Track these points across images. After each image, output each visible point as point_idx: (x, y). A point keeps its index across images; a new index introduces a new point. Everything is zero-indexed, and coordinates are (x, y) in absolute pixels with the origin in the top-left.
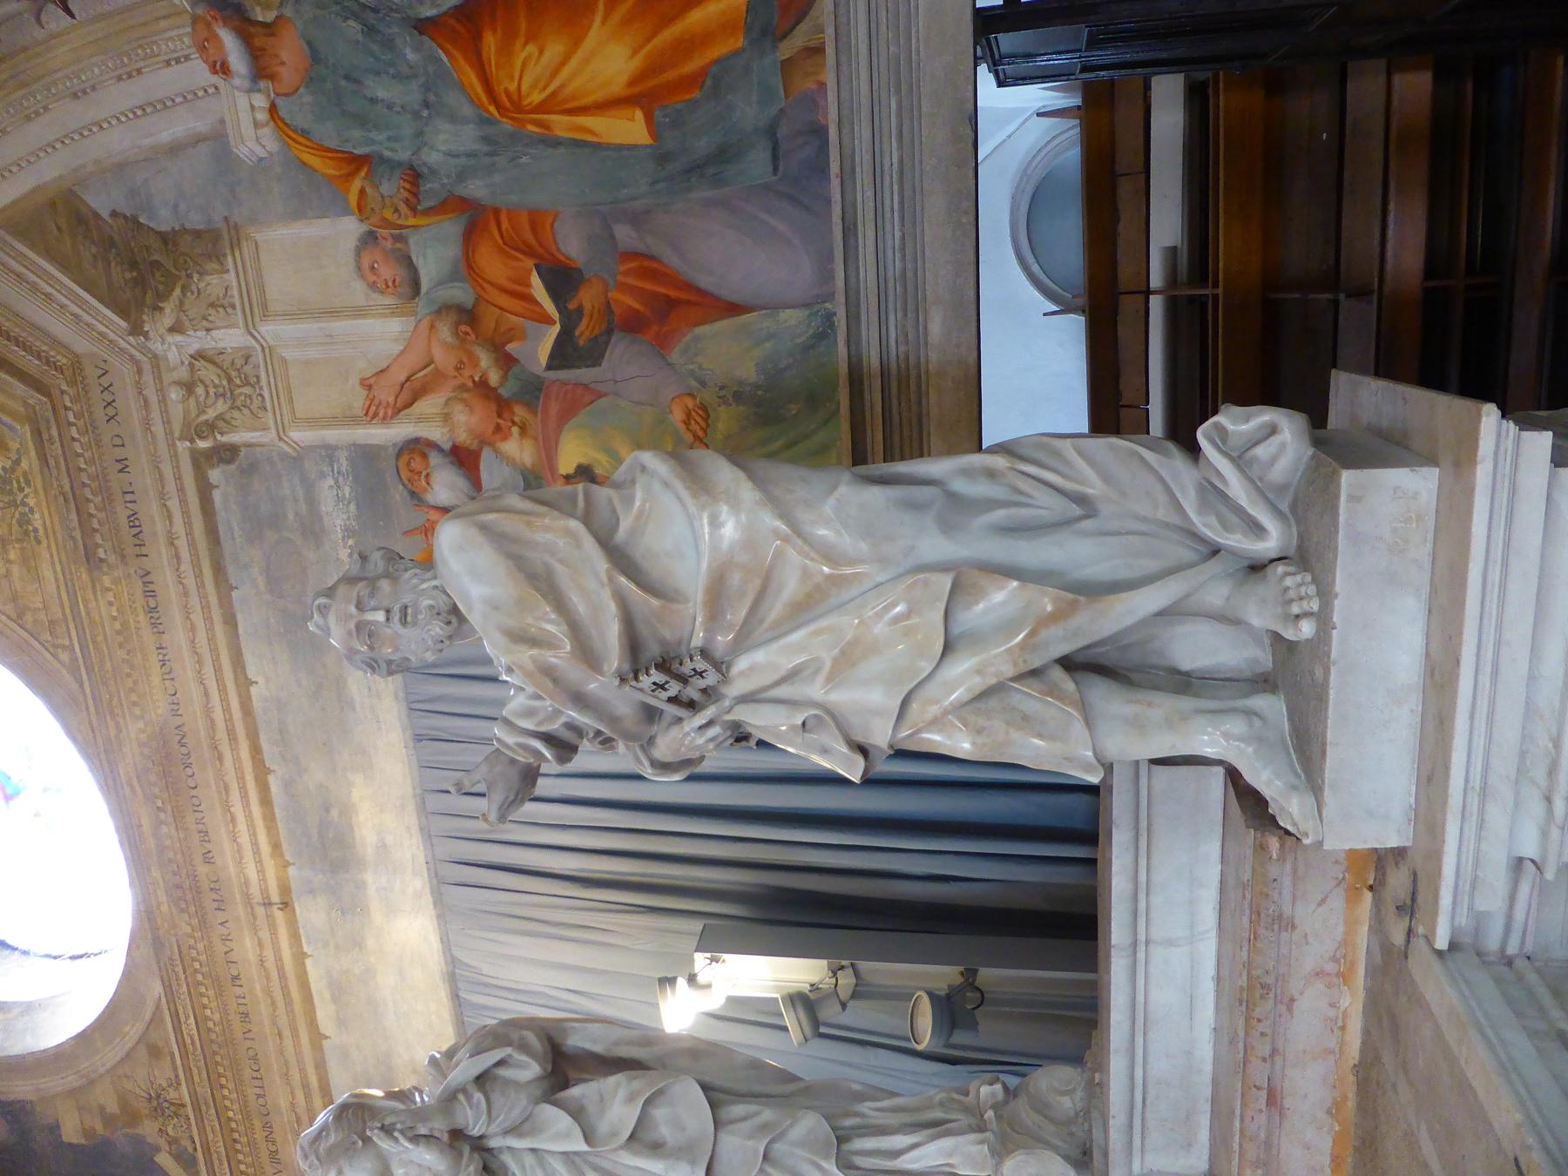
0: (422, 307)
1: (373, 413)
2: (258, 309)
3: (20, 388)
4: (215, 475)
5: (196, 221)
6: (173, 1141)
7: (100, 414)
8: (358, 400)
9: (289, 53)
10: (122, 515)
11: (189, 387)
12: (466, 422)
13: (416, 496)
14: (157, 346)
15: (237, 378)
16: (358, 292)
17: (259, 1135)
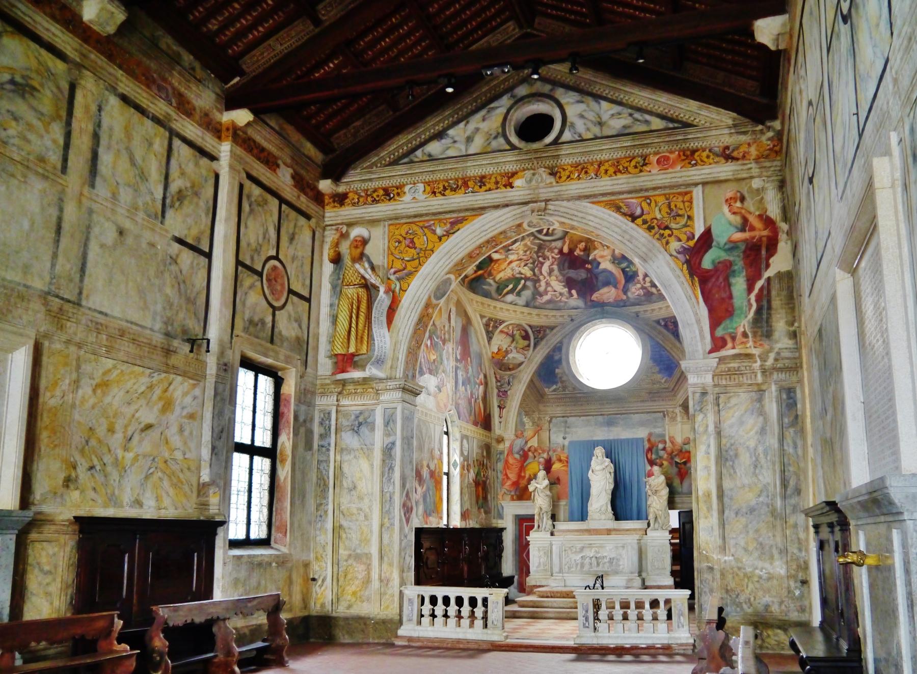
1: (670, 438)
2: (683, 423)
12: (669, 449)
15: (673, 419)
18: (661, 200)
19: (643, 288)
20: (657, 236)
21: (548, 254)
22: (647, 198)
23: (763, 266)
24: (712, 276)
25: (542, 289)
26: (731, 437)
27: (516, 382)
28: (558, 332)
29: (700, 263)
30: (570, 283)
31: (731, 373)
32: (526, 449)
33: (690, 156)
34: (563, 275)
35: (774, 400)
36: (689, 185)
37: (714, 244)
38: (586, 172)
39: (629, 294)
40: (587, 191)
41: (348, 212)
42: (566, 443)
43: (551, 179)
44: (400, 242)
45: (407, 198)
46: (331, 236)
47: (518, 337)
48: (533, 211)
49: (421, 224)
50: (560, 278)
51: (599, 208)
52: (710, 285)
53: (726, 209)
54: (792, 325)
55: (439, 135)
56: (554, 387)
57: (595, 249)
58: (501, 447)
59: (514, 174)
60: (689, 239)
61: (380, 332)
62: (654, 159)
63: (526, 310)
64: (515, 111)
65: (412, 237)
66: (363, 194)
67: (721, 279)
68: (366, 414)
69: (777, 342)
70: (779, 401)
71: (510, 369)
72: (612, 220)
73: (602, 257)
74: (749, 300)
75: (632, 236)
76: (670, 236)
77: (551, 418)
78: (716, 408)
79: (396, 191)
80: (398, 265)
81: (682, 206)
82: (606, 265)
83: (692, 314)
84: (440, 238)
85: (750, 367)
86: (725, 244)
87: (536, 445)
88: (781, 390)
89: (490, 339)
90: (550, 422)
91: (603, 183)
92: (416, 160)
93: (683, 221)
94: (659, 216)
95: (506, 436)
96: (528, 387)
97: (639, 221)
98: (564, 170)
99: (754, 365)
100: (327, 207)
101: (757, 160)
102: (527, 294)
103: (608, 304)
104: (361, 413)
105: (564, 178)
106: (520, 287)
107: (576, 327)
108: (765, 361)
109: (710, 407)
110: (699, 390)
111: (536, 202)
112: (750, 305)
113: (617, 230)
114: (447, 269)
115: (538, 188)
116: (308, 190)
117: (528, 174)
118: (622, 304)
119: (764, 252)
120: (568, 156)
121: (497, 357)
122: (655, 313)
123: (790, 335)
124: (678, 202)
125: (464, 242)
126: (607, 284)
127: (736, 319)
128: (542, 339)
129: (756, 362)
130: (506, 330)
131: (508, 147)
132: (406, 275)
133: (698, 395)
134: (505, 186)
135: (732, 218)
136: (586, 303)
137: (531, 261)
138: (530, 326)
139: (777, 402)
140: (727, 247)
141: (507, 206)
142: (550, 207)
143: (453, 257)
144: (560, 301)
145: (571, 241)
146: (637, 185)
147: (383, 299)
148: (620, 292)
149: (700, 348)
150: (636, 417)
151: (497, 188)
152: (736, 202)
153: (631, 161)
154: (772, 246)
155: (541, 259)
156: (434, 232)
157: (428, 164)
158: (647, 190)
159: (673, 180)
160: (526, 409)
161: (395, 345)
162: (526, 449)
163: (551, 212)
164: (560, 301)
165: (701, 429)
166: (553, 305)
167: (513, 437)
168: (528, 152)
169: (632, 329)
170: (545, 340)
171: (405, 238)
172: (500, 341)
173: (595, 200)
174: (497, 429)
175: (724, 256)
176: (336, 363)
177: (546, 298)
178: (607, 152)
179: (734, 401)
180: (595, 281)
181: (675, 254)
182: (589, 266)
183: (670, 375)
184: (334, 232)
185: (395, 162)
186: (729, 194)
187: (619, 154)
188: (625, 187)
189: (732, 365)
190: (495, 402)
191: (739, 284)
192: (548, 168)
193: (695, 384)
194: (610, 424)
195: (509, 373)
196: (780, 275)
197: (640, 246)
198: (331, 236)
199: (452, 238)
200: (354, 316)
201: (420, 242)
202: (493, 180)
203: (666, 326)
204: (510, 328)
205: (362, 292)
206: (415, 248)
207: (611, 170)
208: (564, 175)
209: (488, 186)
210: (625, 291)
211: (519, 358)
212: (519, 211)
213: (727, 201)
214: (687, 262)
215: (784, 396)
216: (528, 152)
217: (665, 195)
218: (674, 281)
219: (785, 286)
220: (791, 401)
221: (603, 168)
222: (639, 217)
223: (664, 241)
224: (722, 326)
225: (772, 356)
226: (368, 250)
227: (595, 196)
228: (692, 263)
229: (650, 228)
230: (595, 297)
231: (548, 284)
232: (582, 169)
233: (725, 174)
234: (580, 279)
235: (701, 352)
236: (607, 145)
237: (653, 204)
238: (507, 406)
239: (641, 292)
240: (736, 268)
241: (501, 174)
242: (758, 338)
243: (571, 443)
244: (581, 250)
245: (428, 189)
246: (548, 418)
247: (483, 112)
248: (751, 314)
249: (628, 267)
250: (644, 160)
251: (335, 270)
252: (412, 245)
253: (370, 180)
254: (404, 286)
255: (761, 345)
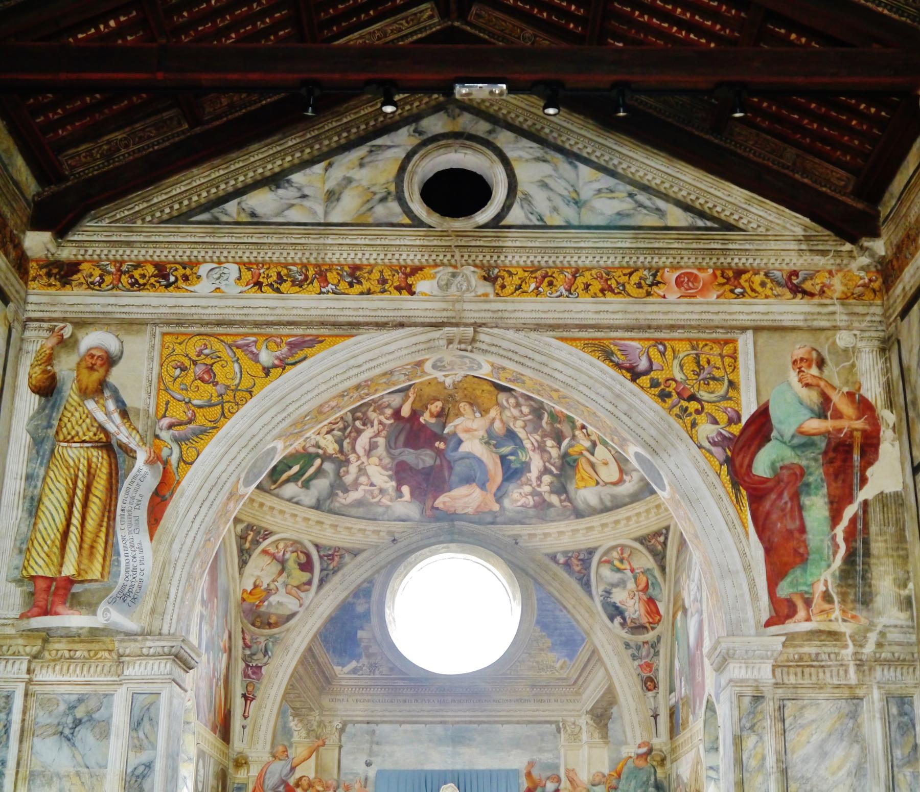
0: (590, 786)
1: (567, 770)
3: (575, 677)
4: (554, 726)
5: (610, 734)
6: (361, 668)
7: (568, 698)
8: (570, 767)
9: (641, 763)
10: (545, 698)
11: (574, 724)
13: (548, 778)
14: (583, 717)
15: (575, 737)
16: (593, 771)
17: (367, 698)
18: (684, 349)
19: (534, 493)
20: (676, 410)
21: (372, 415)
22: (660, 341)
23: (856, 480)
24: (770, 490)
25: (349, 479)
26: (805, 780)
27: (277, 651)
28: (367, 560)
29: (750, 466)
30: (401, 473)
31: (802, 664)
32: (292, 782)
33: (733, 280)
34: (392, 457)
35: (878, 715)
36: (732, 329)
37: (774, 434)
38: (551, 284)
39: (507, 503)
40: (551, 318)
41: (76, 299)
42: (372, 773)
43: (487, 288)
44: (183, 369)
45: (203, 287)
46: (37, 341)
47: (292, 565)
48: (450, 342)
49: (229, 340)
50: (387, 461)
51: (574, 350)
52: (767, 505)
53: (793, 376)
54: (905, 586)
55: (275, 180)
56: (354, 664)
57: (459, 414)
58: (241, 776)
59: (416, 270)
60: (731, 421)
61: (131, 535)
62: (671, 276)
63: (314, 515)
64: (423, 157)
65: (209, 361)
66: (112, 269)
67: (786, 497)
68: (93, 703)
69: (880, 614)
70: (887, 721)
71: (270, 625)
72: (595, 372)
73: (468, 431)
74: (834, 538)
75: (630, 405)
76: (698, 412)
77: (345, 724)
78: (780, 725)
79: (181, 271)
80: (178, 412)
81: (719, 363)
82: (473, 446)
83: (736, 554)
84: (267, 371)
85: (837, 654)
86: (793, 437)
87: (312, 775)
88: (888, 698)
89: (243, 563)
90: (342, 731)
91: (580, 307)
92: (225, 219)
93: (722, 389)
94: (679, 376)
95: (252, 755)
96: (303, 661)
97: (645, 380)
98: (510, 274)
99: (844, 652)
100: (32, 284)
101: (844, 299)
102: (321, 485)
103: (464, 517)
104: (80, 700)
105: (510, 289)
106: (311, 470)
107: (401, 554)
108: (861, 646)
109: (768, 723)
110: (749, 692)
111: (457, 325)
112: (836, 547)
113: (603, 391)
114: (277, 430)
115: (460, 300)
116: (10, 247)
117: (444, 273)
118: (489, 519)
119: (856, 456)
120: (517, 251)
121: (251, 600)
122: (550, 541)
123: (901, 603)
124: (712, 354)
125: (314, 382)
126: (468, 480)
127: (811, 569)
128: (335, 572)
129: (846, 646)
130: (272, 550)
131: (407, 221)
132: (193, 434)
133: (746, 701)
134: (399, 289)
135: (804, 392)
136: (422, 512)
137: (341, 425)
138: (317, 546)
139: (883, 719)
140: (796, 441)
141: (402, 325)
142: (482, 337)
143: (291, 409)
144: (378, 504)
145: (419, 396)
146: (642, 317)
147: (142, 476)
148: (490, 498)
149: (750, 615)
150: (507, 731)
151: (383, 291)
152: (810, 366)
153: (631, 274)
154: (870, 446)
155: (358, 424)
156: (255, 358)
157: (250, 229)
158: (659, 328)
159: (704, 316)
160: (295, 702)
161: (164, 569)
162: (292, 782)
163: (484, 347)
164: (378, 504)
165: (753, 763)
166: (365, 510)
167: (267, 757)
168: (445, 234)
169: (505, 566)
170: (340, 574)
171: (195, 363)
172: (260, 569)
173: (565, 334)
174: (238, 743)
175: (790, 457)
176: (32, 594)
177: (354, 496)
178: (590, 252)
179: (810, 714)
180: (446, 474)
181: (706, 444)
182: (441, 445)
183: (571, 656)
184: (46, 334)
185: (183, 218)
186: (800, 353)
187: (611, 261)
188: (619, 319)
189: (806, 650)
190: (238, 689)
191: (816, 508)
192: (482, 267)
193: (742, 681)
194: (458, 740)
195: (267, 631)
196: (882, 498)
197: (645, 425)
198: (37, 341)
199: (292, 372)
200: (78, 504)
201: (227, 373)
202: (376, 275)
203: (567, 565)
204: (281, 546)
205: (99, 458)
206: (216, 384)
207: (596, 286)
208: (511, 283)
209: (366, 285)
210: (499, 499)
211: (291, 604)
212: (423, 338)
213: (795, 362)
214: (729, 461)
215: (894, 710)
216: (445, 234)
217: (690, 340)
218: (705, 491)
219: (892, 516)
220: (906, 719)
221: (580, 281)
222: (646, 373)
223: (688, 420)
224: (788, 579)
225: (873, 637)
226: (116, 376)
227: (566, 327)
228: (737, 463)
229: (664, 396)
230: (442, 501)
231: (362, 470)
232: (544, 277)
233: (790, 317)
234: (421, 466)
235: (752, 622)
236: (590, 240)
237: (669, 353)
238: (259, 695)
239: (530, 501)
240: (811, 479)
241: (391, 267)
242: (850, 606)
243: (380, 773)
244: (432, 415)
245: (247, 275)
246: (337, 723)
247: (362, 151)
248: (838, 562)
249: (512, 454)
250: (655, 275)
251: (42, 408)
252: (209, 376)
253: (129, 244)
254: (190, 454)
255: (854, 617)
